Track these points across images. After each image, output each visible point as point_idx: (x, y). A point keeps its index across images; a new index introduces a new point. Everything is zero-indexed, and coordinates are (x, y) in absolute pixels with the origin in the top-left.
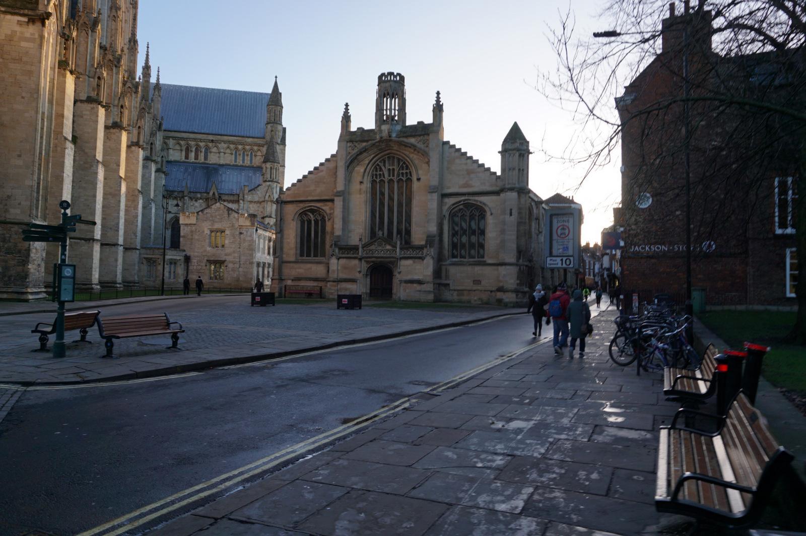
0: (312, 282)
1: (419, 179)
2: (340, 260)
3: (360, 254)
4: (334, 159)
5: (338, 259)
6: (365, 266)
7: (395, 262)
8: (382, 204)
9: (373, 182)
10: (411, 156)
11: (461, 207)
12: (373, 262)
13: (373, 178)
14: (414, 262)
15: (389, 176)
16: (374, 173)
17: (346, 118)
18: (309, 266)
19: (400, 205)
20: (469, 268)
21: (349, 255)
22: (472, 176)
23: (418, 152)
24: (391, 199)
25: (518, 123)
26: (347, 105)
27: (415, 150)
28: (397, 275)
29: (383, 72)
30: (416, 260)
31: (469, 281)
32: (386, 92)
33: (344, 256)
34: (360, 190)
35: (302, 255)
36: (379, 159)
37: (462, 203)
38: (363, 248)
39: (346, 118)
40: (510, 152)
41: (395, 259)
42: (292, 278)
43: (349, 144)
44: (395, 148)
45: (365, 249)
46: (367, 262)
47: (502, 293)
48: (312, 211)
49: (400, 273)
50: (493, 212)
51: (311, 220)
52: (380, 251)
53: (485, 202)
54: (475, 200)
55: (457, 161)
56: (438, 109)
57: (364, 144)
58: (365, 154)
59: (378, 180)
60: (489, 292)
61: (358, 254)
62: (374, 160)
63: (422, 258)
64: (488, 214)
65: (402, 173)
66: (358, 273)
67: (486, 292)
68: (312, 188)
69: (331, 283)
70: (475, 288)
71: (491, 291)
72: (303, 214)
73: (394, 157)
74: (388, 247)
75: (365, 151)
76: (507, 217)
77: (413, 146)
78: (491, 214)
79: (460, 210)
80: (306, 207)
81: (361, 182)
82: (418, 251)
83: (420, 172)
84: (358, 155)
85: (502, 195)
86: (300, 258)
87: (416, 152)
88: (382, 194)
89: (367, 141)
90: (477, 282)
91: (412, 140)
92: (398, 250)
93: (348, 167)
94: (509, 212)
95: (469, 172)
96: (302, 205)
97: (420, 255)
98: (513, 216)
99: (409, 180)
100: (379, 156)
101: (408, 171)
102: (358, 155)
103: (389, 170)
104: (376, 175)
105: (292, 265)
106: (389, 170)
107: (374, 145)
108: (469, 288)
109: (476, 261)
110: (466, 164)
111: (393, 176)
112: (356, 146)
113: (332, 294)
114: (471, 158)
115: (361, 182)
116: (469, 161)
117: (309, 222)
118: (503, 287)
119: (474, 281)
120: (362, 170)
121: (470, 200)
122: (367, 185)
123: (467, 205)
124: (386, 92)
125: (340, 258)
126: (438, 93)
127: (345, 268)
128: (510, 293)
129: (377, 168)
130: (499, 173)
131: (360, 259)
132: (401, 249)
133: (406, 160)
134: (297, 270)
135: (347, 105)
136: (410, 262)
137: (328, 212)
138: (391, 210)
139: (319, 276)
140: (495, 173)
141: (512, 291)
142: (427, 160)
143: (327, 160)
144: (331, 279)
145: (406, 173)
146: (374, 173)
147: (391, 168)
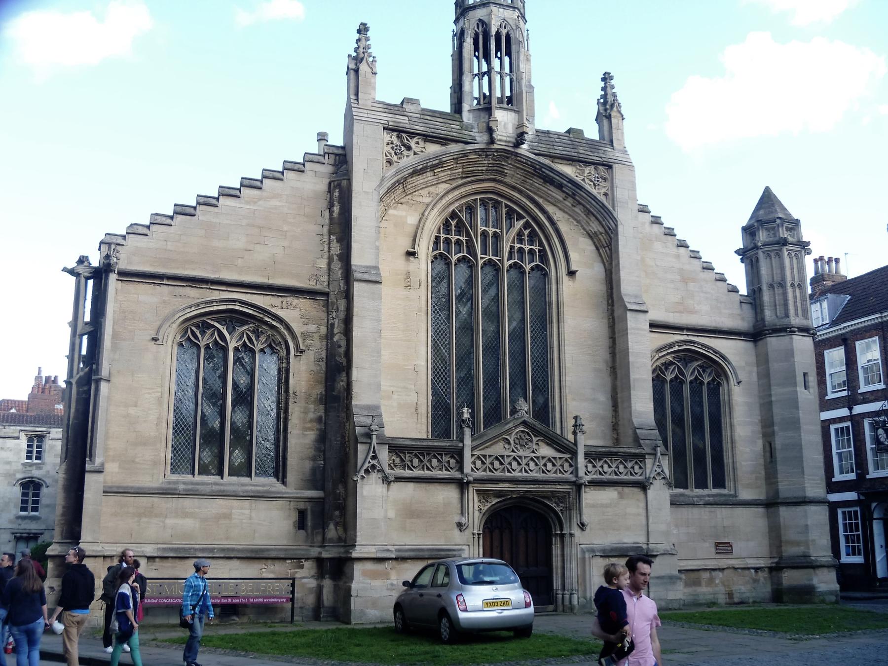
0: (236, 563)
1: (571, 273)
2: (395, 486)
3: (467, 468)
5: (389, 483)
6: (476, 510)
10: (550, 209)
11: (670, 358)
12: (498, 494)
14: (621, 496)
15: (484, 252)
16: (443, 236)
17: (359, 65)
18: (219, 505)
19: (518, 336)
20: (704, 514)
21: (427, 473)
22: (691, 286)
24: (494, 315)
25: (775, 191)
26: (363, 29)
28: (576, 531)
30: (627, 490)
31: (707, 545)
32: (504, 32)
33: (407, 473)
34: (408, 275)
37: (676, 348)
38: (473, 449)
39: (359, 65)
40: (767, 249)
41: (567, 487)
43: (387, 137)
44: (508, 180)
45: (476, 453)
46: (484, 495)
47: (811, 571)
48: (233, 318)
49: (582, 526)
50: (742, 376)
51: (225, 350)
53: (723, 351)
54: (704, 346)
55: (658, 246)
57: (433, 149)
58: (429, 176)
59: (454, 258)
60: (753, 571)
61: (461, 469)
62: (450, 196)
63: (643, 486)
64: (733, 381)
65: (521, 250)
66: (456, 531)
67: (747, 572)
68: (238, 242)
69: (369, 566)
70: (724, 562)
71: (757, 569)
73: (497, 205)
74: (546, 451)
75: (433, 167)
76: (800, 389)
79: (667, 365)
80: (212, 302)
81: (411, 254)
82: (629, 465)
83: (573, 256)
84: (416, 173)
85: (774, 342)
86: (175, 477)
87: (569, 203)
88: (468, 296)
89: (443, 140)
90: (723, 548)
91: (568, 170)
92: (581, 459)
93: (381, 199)
94: (800, 379)
95: (686, 279)
96: (195, 294)
97: (637, 478)
98: (811, 390)
99: (542, 272)
100: (462, 190)
101: (536, 248)
102: (416, 173)
104: (447, 241)
105: (144, 501)
106: (484, 234)
107: (465, 155)
108: (712, 564)
109: (713, 496)
110: (678, 256)
112: (409, 148)
113: (374, 604)
114: (682, 244)
115: (411, 254)
116: (682, 250)
118: (806, 556)
119: (718, 545)
120: (412, 219)
121: (694, 342)
122: (423, 266)
123: (687, 356)
124: (504, 32)
125: (398, 479)
126: (607, 78)
127: (411, 513)
128: (825, 570)
129: (454, 223)
131: (462, 485)
132: (587, 455)
133: (536, 219)
134: (170, 522)
136: (609, 495)
137: (297, 327)
138: (493, 349)
139: (260, 541)
140: (734, 290)
141: (828, 567)
142: (595, 227)
143: (290, 167)
144: (372, 552)
145: (531, 251)
146: (443, 236)
147: (491, 230)
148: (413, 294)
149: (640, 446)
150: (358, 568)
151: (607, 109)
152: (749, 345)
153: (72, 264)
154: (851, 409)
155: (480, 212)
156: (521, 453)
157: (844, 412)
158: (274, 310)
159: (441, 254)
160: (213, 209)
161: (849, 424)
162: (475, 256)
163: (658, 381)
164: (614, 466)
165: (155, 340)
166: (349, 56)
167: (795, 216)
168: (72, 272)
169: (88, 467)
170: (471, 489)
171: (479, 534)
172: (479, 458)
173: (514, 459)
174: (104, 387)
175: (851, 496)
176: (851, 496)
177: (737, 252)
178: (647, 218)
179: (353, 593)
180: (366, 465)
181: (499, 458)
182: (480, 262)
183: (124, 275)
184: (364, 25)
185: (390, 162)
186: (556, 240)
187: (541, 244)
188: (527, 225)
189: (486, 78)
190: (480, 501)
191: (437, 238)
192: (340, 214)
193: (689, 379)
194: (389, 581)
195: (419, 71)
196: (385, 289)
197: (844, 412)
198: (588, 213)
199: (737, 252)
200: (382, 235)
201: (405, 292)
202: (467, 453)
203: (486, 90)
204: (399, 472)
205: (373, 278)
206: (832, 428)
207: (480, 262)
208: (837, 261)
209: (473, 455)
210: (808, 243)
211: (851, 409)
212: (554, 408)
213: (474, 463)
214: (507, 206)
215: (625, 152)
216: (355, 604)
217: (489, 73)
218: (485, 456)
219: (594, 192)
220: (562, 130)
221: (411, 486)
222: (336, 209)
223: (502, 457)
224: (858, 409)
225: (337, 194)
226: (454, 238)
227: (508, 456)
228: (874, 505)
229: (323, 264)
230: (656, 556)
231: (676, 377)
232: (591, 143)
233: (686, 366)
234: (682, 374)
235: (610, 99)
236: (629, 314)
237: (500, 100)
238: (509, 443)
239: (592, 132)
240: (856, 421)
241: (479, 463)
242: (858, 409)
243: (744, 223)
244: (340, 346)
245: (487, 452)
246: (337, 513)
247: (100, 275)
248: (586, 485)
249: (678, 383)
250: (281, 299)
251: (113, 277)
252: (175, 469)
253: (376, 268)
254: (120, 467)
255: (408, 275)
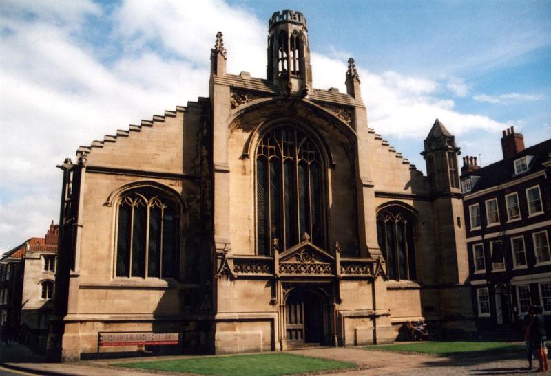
2: (238, 282)
4: (195, 110)
7: (334, 283)
8: (278, 196)
9: (262, 160)
13: (259, 152)
16: (263, 146)
21: (255, 274)
23: (335, 128)
27: (330, 124)
29: (277, 11)
32: (295, 36)
33: (244, 274)
34: (244, 167)
35: (122, 271)
36: (271, 126)
42: (106, 317)
46: (285, 286)
48: (150, 191)
52: (308, 267)
56: (351, 79)
63: (371, 281)
64: (420, 223)
72: (129, 194)
77: (334, 121)
78: (423, 223)
87: (332, 127)
88: (277, 179)
93: (229, 127)
96: (129, 179)
103: (285, 144)
104: (265, 149)
105: (103, 292)
111: (293, 154)
112: (244, 99)
117: (141, 210)
122: (251, 163)
124: (295, 36)
125: (240, 278)
127: (247, 295)
130: (425, 174)
132: (343, 263)
134: (116, 302)
135: (219, 35)
136: (354, 284)
142: (346, 140)
146: (263, 146)
147: (289, 143)
148: (247, 177)
149: (370, 257)
150: (219, 326)
151: (351, 79)
152: (429, 203)
153: (62, 163)
154: (483, 237)
155: (283, 134)
156: (309, 262)
157: (479, 238)
158: (171, 187)
159: (262, 156)
160: (138, 133)
161: (482, 244)
162: (280, 156)
163: (380, 223)
164: (356, 269)
165: (106, 204)
166: (212, 50)
167: (452, 135)
168: (61, 167)
169: (72, 273)
170: (279, 282)
171: (284, 306)
172: (283, 265)
173: (302, 266)
174: (79, 230)
175: (484, 282)
176: (484, 282)
177: (422, 154)
178: (373, 136)
179: (216, 338)
180: (222, 270)
181: (295, 266)
182: (283, 160)
183: (92, 170)
184: (220, 32)
185: (233, 107)
186: (324, 148)
187: (316, 150)
188: (308, 140)
189: (285, 62)
190: (284, 288)
191: (260, 148)
192: (207, 134)
193: (397, 221)
194: (235, 333)
195: (250, 59)
196: (232, 175)
197: (479, 238)
198: (341, 132)
199: (422, 154)
200: (230, 146)
201: (244, 177)
202: (277, 262)
203: (286, 67)
204: (240, 274)
205: (224, 169)
206: (474, 246)
207: (283, 160)
208: (475, 158)
209: (280, 264)
210: (459, 149)
211: (483, 237)
212: (324, 237)
213: (280, 268)
214: (297, 130)
215: (361, 101)
216: (218, 344)
217: (287, 58)
218: (286, 264)
219: (345, 122)
220: (327, 88)
221: (246, 282)
222: (205, 132)
223: (296, 264)
224: (487, 236)
225: (205, 124)
226: (269, 147)
227: (299, 264)
228: (495, 286)
229: (198, 162)
230: (378, 316)
231: (390, 220)
232: (343, 95)
233: (395, 215)
234: (393, 219)
235: (353, 73)
236: (364, 188)
237: (293, 73)
238: (299, 257)
239: (343, 90)
240: (486, 242)
241: (283, 268)
242: (487, 236)
243: (425, 138)
244: (207, 206)
245: (288, 262)
246: (207, 296)
247: (77, 169)
248: (342, 280)
249: (391, 223)
250: (175, 181)
251: (84, 170)
252: (118, 274)
253: (227, 163)
254: (89, 272)
255: (244, 167)
